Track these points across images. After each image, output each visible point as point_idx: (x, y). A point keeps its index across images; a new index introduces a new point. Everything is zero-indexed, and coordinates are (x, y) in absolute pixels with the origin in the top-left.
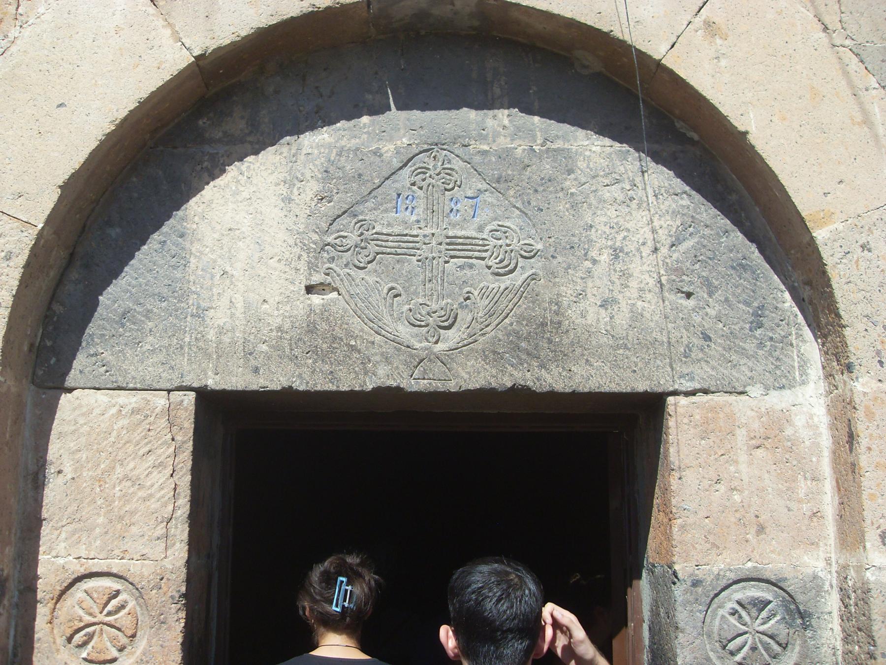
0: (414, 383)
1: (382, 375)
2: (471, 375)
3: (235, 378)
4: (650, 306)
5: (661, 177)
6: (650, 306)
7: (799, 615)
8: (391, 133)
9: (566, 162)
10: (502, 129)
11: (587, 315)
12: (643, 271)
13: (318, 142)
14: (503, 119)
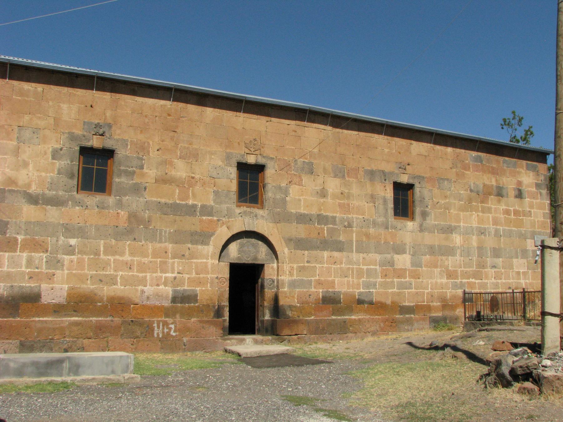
0: (246, 262)
1: (244, 262)
2: (250, 262)
3: (233, 262)
4: (264, 257)
5: (265, 246)
6: (264, 257)
7: (273, 282)
8: (244, 241)
9: (258, 244)
10: (253, 241)
11: (259, 257)
12: (264, 254)
13: (239, 241)
14: (253, 240)
